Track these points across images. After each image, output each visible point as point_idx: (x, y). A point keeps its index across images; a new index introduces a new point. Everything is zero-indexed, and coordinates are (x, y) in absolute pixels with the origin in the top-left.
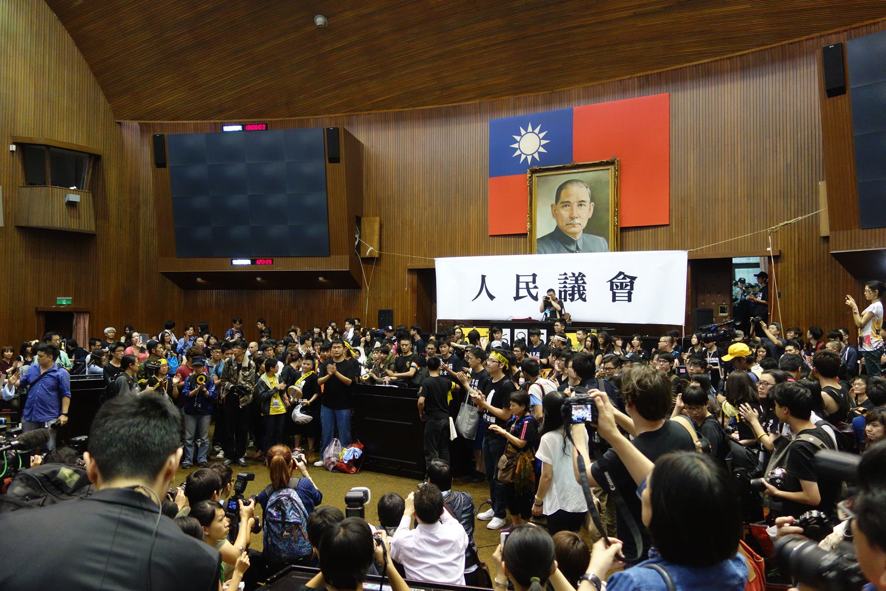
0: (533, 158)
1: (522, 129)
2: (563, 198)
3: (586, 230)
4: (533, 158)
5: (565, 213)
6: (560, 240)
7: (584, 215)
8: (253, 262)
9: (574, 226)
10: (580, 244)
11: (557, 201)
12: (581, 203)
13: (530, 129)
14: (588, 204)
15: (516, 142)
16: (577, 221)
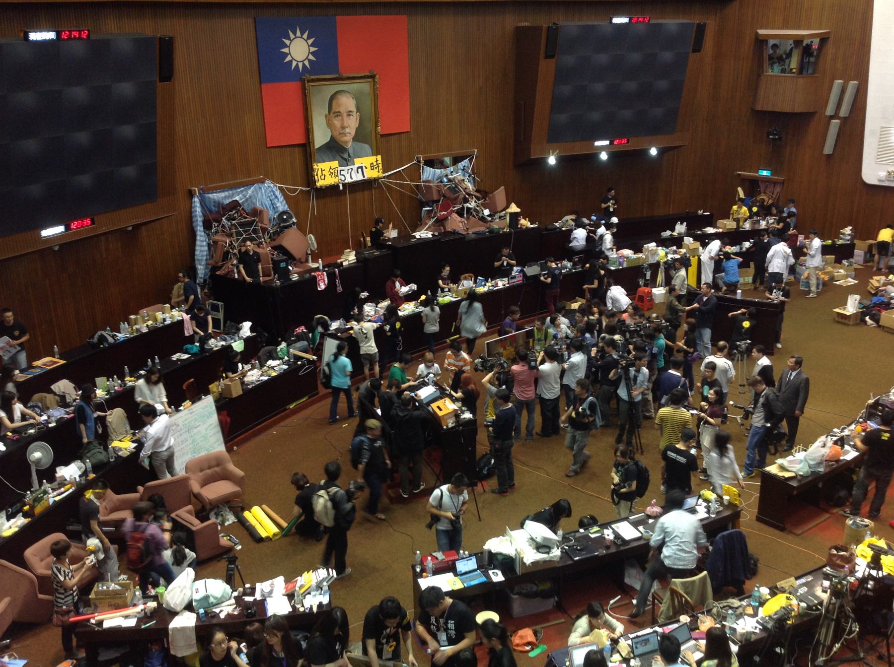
0: (304, 64)
1: (291, 33)
2: (335, 109)
3: (355, 139)
4: (304, 64)
5: (337, 122)
6: (335, 149)
7: (352, 124)
8: (68, 228)
9: (345, 134)
10: (351, 151)
11: (329, 112)
12: (349, 114)
13: (298, 34)
14: (354, 114)
15: (286, 46)
16: (347, 130)
